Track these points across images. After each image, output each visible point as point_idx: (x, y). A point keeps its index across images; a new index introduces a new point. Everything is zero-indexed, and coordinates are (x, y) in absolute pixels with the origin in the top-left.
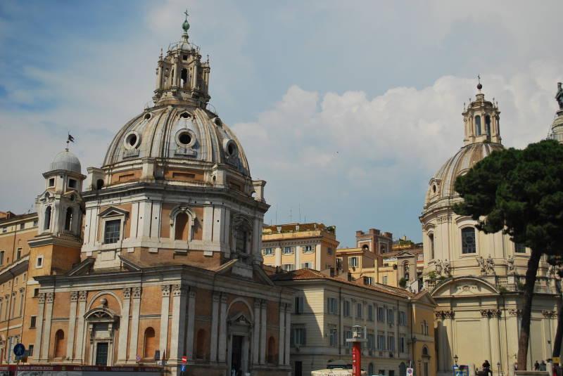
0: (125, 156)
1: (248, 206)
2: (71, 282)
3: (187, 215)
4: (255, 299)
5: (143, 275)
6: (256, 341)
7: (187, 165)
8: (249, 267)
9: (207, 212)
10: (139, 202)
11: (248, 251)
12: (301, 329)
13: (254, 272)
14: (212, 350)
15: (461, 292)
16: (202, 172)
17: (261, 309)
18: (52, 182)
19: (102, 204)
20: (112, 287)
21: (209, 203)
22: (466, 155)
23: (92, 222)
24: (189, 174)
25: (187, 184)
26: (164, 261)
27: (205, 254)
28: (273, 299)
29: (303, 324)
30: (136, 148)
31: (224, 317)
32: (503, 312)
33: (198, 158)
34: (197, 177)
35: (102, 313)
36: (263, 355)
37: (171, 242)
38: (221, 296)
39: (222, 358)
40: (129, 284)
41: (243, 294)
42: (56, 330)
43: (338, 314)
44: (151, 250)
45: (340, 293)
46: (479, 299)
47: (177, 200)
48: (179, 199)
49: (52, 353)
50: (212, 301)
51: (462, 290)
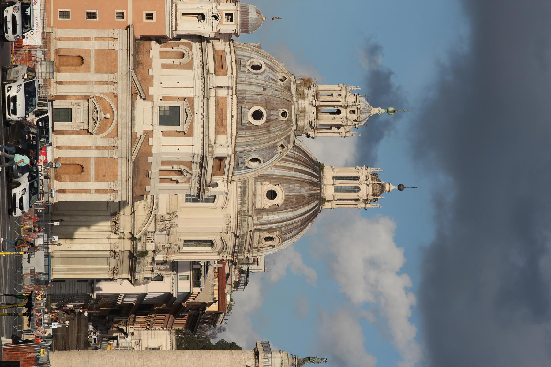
0: (243, 110)
20: (119, 125)
22: (308, 187)
32: (117, 236)
35: (97, 118)
40: (122, 143)
49: (61, 54)
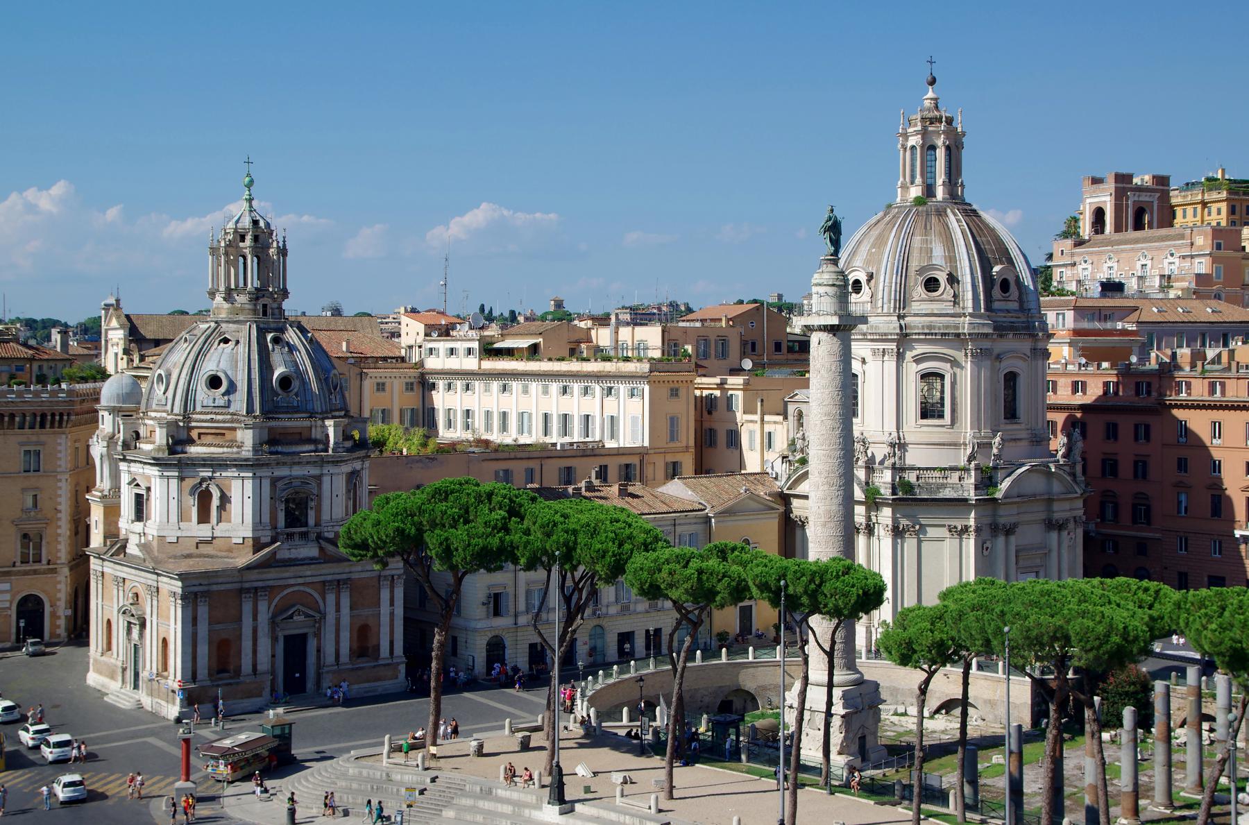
7: (218, 422)
16: (234, 429)
26: (186, 552)
27: (234, 541)
33: (231, 410)
34: (229, 435)
41: (300, 581)
44: (169, 540)
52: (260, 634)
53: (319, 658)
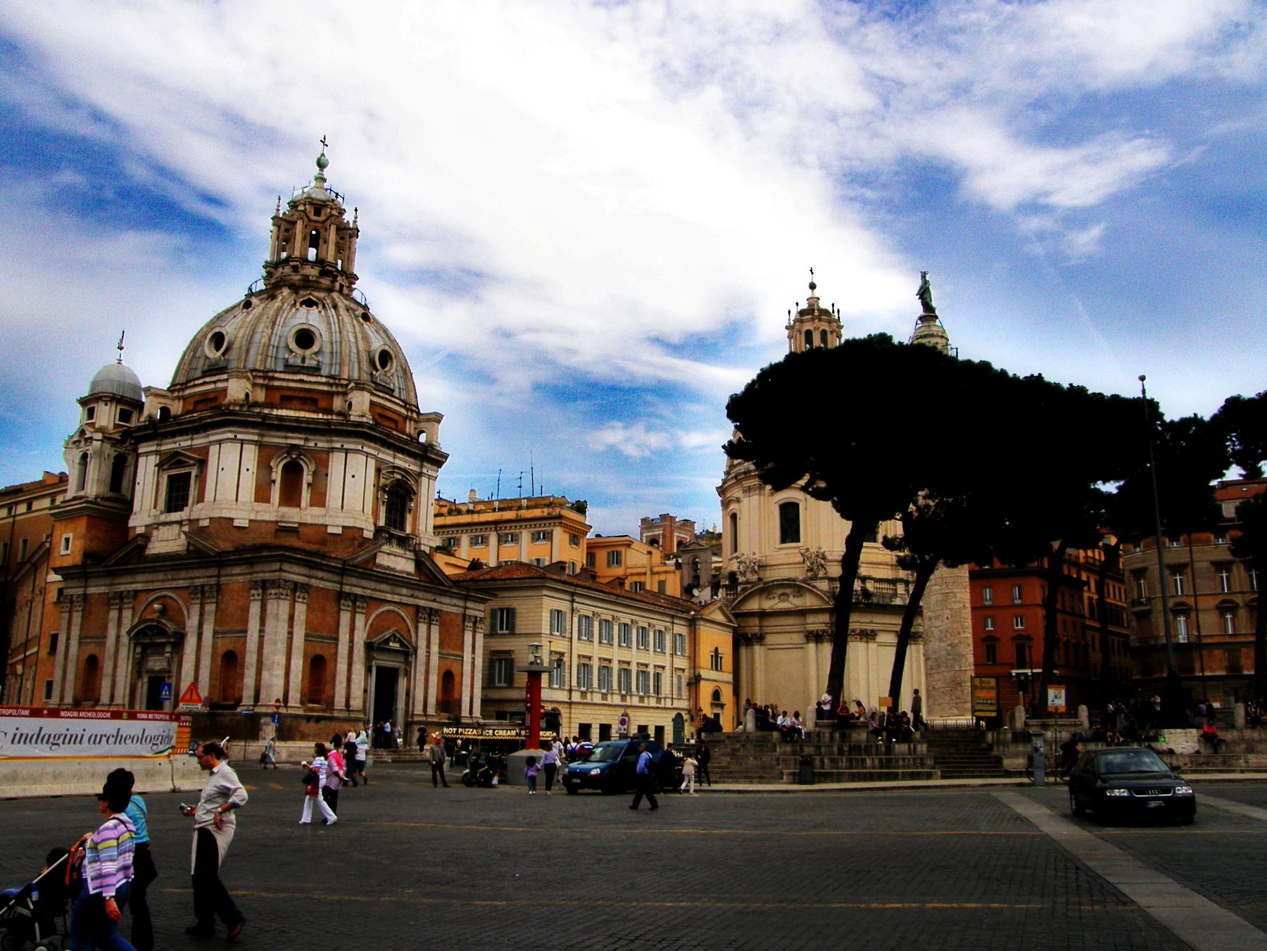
1: (410, 454)
2: (112, 574)
3: (301, 469)
4: (417, 607)
5: (220, 561)
6: (420, 677)
8: (410, 555)
9: (336, 460)
10: (220, 442)
11: (408, 530)
12: (506, 660)
13: (419, 564)
14: (337, 689)
15: (769, 604)
16: (331, 395)
17: (430, 625)
18: (91, 413)
19: (163, 448)
20: (174, 584)
21: (339, 445)
23: (148, 479)
24: (308, 399)
25: (302, 414)
26: (259, 541)
27: (330, 530)
28: (454, 610)
29: (509, 652)
30: (223, 354)
31: (361, 637)
33: (325, 371)
36: (432, 700)
37: (272, 511)
38: (354, 602)
39: (356, 703)
40: (201, 577)
41: (397, 598)
42: (86, 656)
43: (568, 635)
44: (236, 523)
45: (573, 601)
46: (802, 613)
47: (283, 441)
48: (286, 438)
50: (340, 610)
51: (777, 600)
52: (355, 658)
53: (407, 703)
